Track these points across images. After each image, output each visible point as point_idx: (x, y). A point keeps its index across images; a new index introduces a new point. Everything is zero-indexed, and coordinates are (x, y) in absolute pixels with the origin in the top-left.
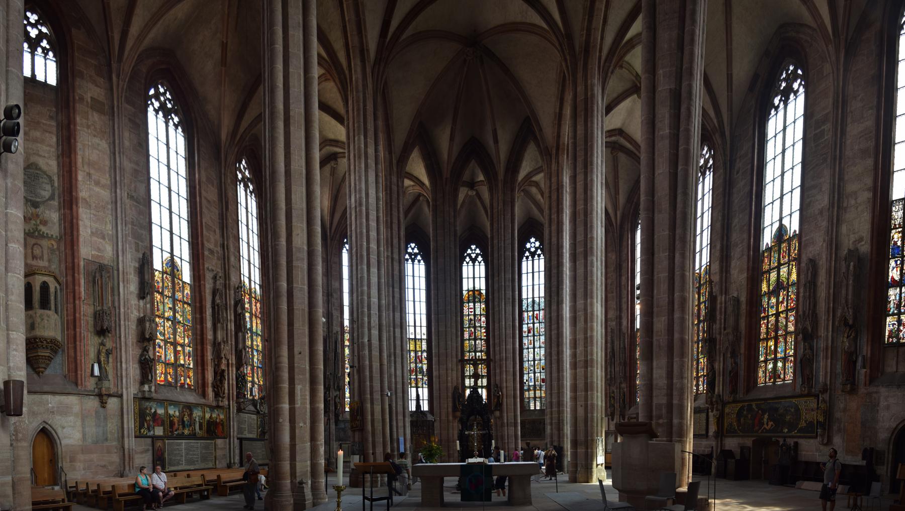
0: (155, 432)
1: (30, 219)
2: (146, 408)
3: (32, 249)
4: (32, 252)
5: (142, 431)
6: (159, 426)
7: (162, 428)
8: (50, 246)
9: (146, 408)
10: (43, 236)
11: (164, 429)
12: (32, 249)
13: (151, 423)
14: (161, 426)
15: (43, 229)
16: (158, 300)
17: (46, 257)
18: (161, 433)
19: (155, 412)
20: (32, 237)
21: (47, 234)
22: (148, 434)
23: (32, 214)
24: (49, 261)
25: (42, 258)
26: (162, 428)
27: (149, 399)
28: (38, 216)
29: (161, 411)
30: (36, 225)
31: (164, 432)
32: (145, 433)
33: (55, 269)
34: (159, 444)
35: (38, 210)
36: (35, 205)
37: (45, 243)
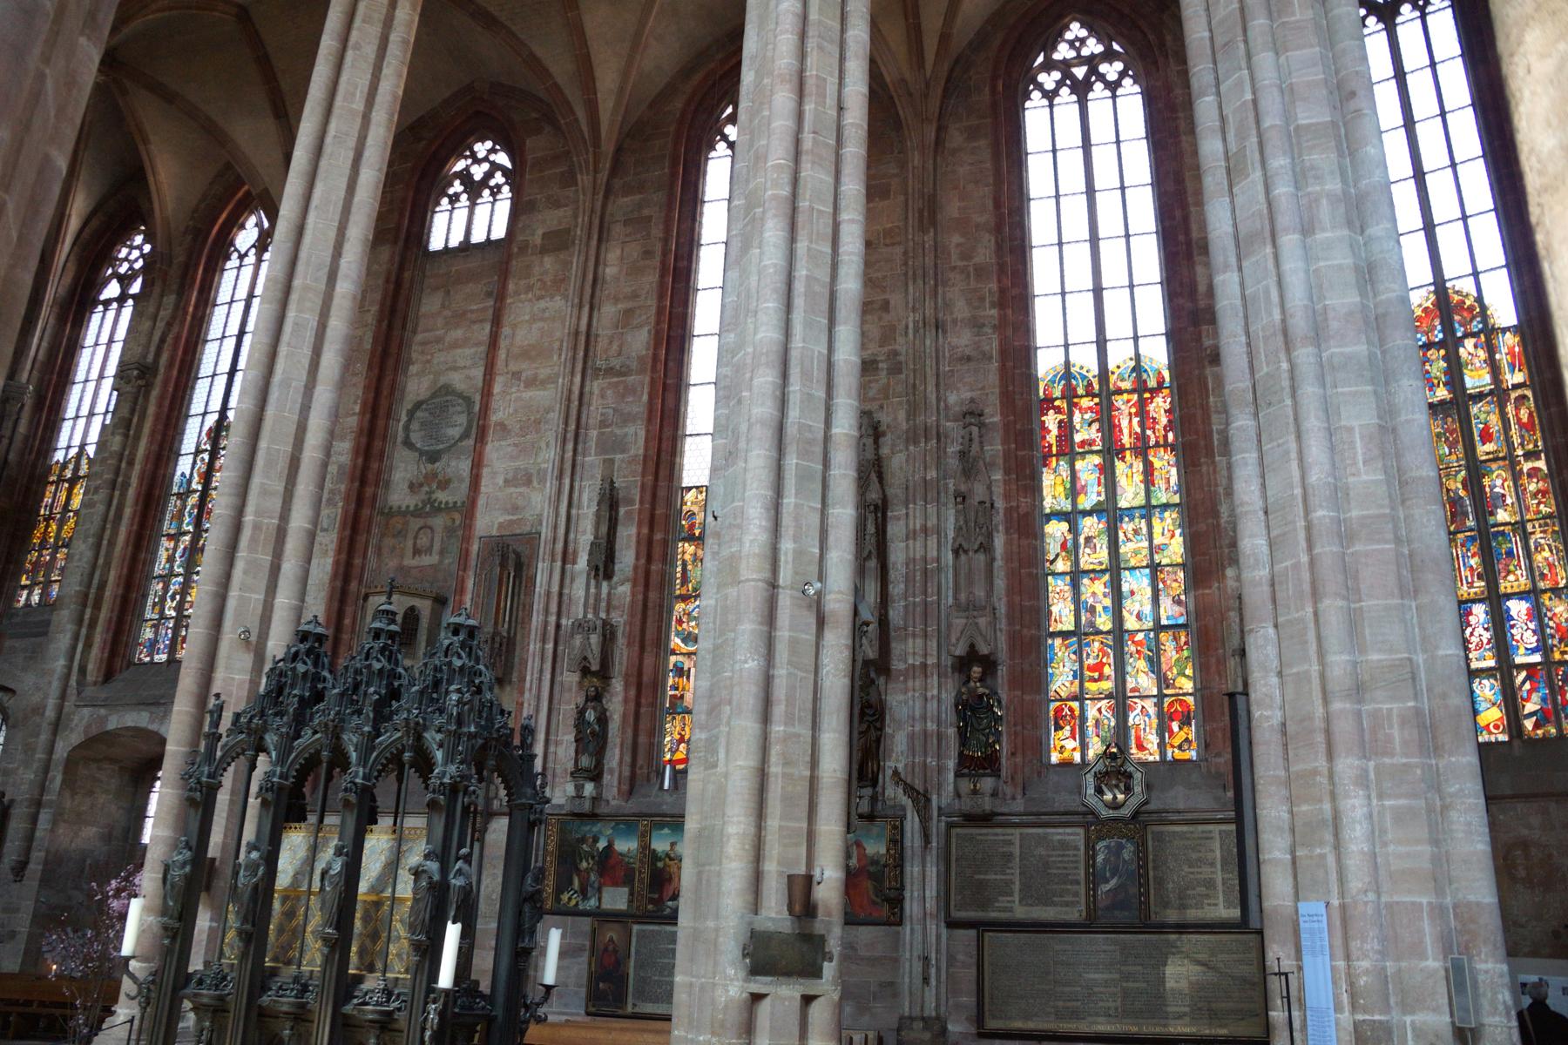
0: (603, 900)
1: (421, 485)
2: (583, 840)
3: (416, 538)
4: (415, 544)
5: (565, 897)
6: (615, 884)
7: (626, 890)
8: (449, 523)
9: (583, 840)
10: (438, 509)
11: (631, 894)
12: (416, 538)
13: (593, 877)
14: (624, 884)
15: (442, 496)
16: (687, 557)
17: (437, 547)
18: (622, 905)
19: (610, 847)
20: (419, 516)
21: (447, 503)
22: (581, 907)
23: (426, 477)
24: (442, 553)
25: (429, 550)
26: (626, 890)
27: (593, 817)
28: (435, 475)
29: (626, 845)
30: (431, 493)
31: (630, 902)
32: (573, 902)
33: (450, 564)
34: (611, 933)
35: (437, 464)
36: (433, 457)
37: (439, 522)
